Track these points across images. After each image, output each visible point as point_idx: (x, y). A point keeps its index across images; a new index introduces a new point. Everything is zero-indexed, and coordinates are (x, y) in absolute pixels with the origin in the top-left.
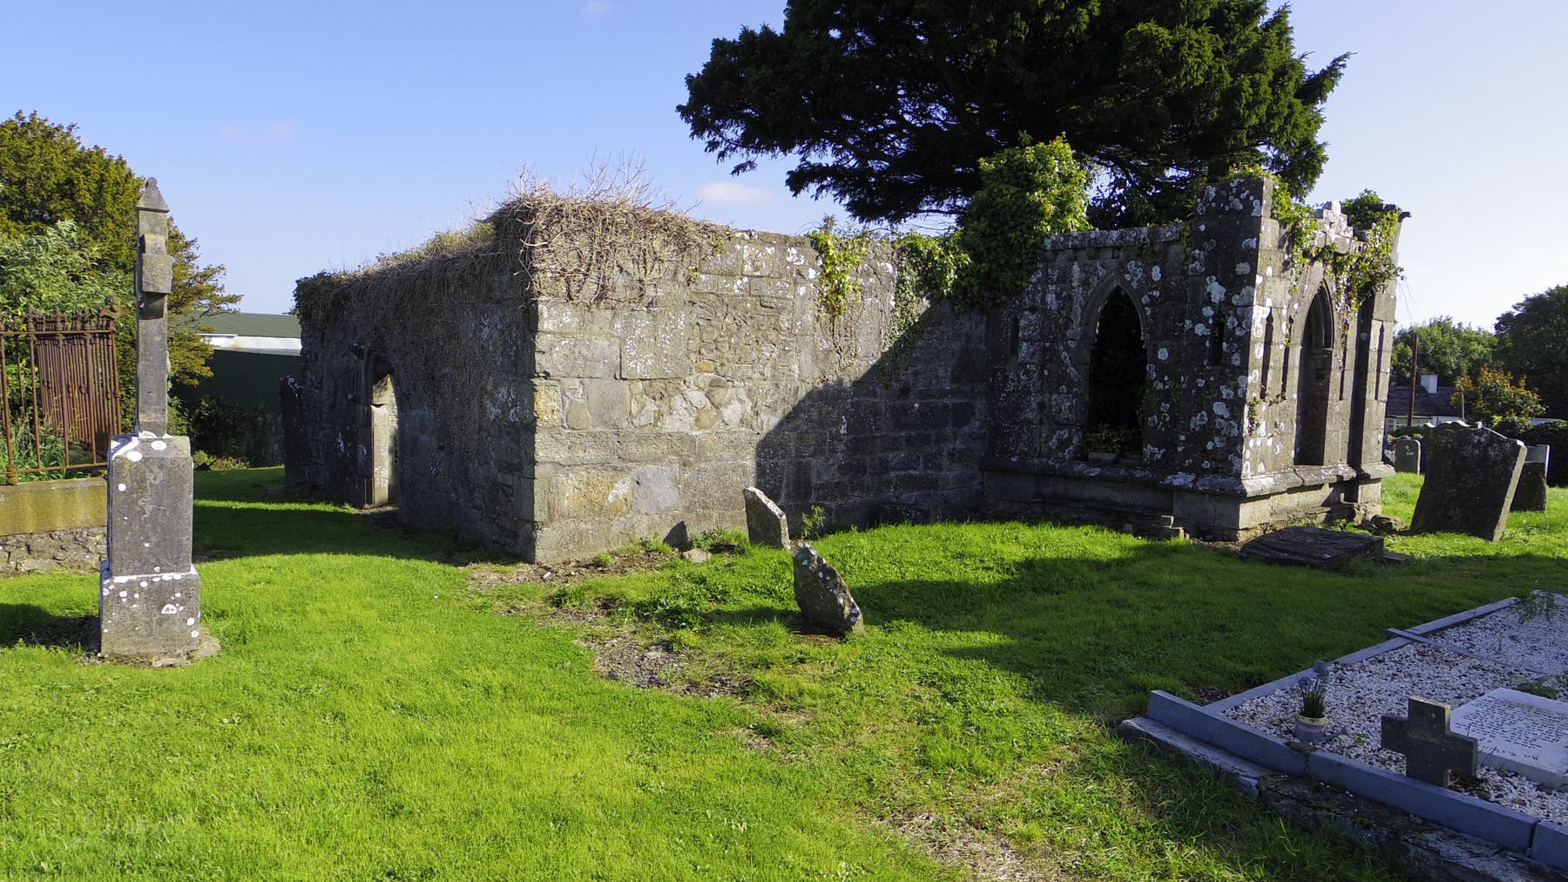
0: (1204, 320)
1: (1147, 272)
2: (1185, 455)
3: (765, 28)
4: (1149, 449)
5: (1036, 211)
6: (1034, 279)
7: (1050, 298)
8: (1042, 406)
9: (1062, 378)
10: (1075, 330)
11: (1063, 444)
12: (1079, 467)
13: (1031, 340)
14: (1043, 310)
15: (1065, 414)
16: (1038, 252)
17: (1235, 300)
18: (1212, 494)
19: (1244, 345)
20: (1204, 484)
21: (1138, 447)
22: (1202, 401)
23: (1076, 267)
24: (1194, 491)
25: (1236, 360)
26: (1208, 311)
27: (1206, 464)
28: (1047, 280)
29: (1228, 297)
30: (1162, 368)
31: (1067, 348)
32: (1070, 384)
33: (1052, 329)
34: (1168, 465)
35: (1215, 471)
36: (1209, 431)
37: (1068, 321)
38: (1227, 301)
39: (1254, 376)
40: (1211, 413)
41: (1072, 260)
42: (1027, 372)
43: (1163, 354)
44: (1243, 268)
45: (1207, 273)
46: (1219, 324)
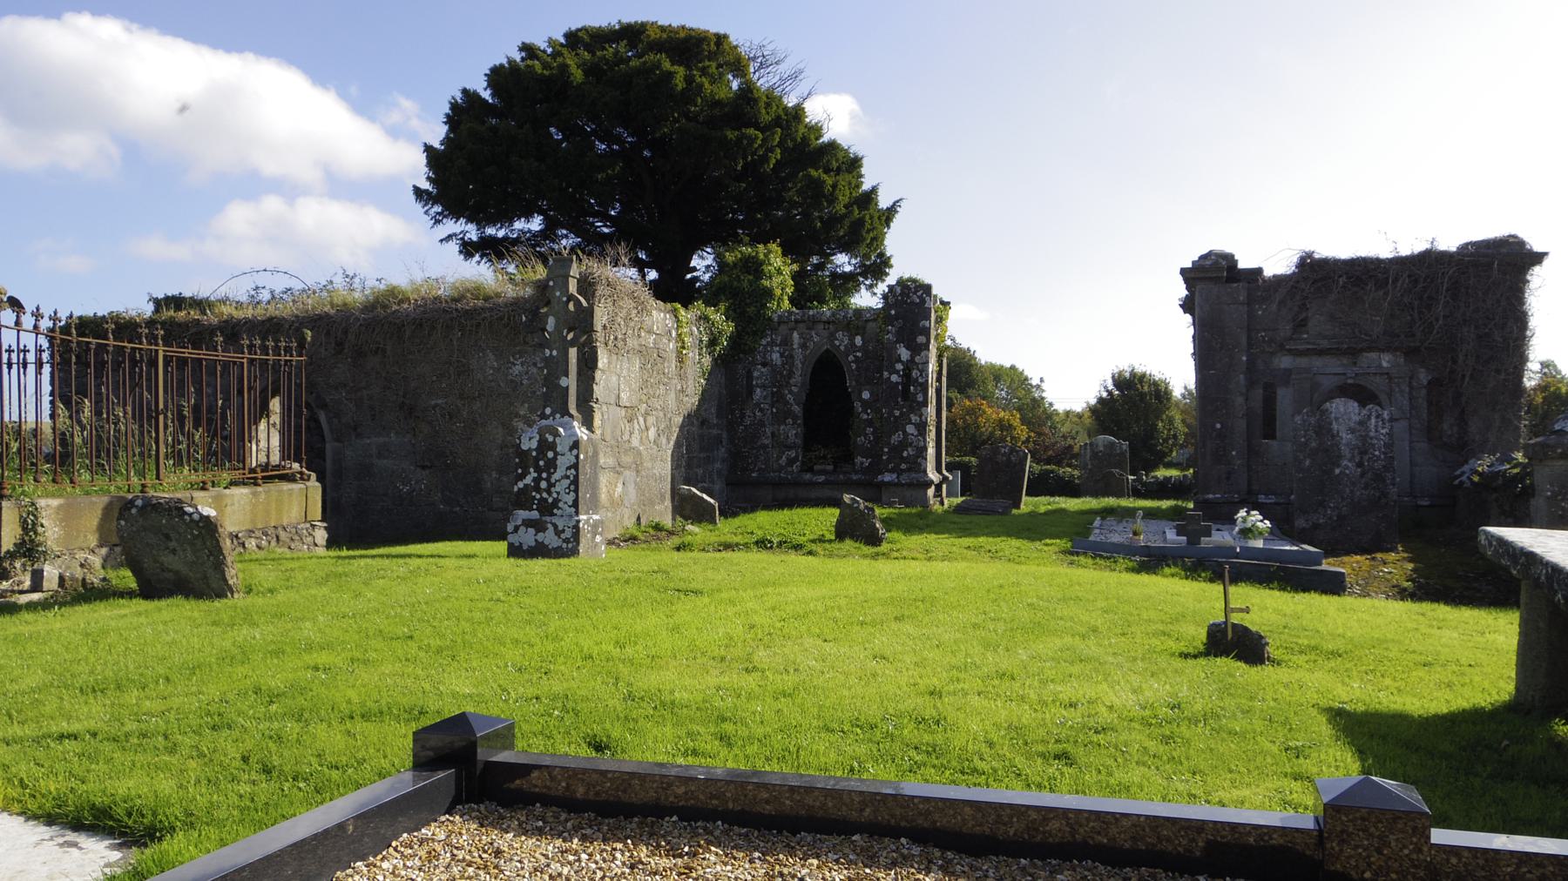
0: (897, 372)
1: (852, 340)
2: (889, 461)
3: (465, 91)
4: (859, 459)
5: (768, 293)
6: (764, 342)
7: (776, 356)
8: (773, 434)
9: (789, 414)
10: (797, 378)
11: (791, 462)
12: (808, 476)
13: (764, 387)
14: (773, 367)
15: (792, 438)
16: (770, 325)
17: (917, 359)
18: (910, 485)
19: (924, 387)
20: (904, 479)
21: (848, 458)
22: (899, 424)
23: (795, 335)
24: (898, 485)
25: (920, 398)
26: (899, 367)
27: (903, 466)
28: (773, 343)
29: (912, 357)
30: (865, 404)
31: (791, 392)
32: (795, 418)
33: (779, 379)
34: (877, 467)
35: (909, 470)
36: (904, 444)
37: (791, 374)
38: (912, 361)
39: (931, 410)
40: (905, 432)
41: (793, 329)
42: (761, 410)
43: (866, 395)
44: (921, 339)
45: (898, 342)
46: (907, 375)
